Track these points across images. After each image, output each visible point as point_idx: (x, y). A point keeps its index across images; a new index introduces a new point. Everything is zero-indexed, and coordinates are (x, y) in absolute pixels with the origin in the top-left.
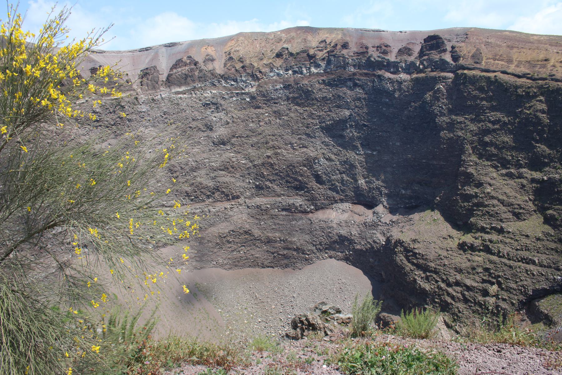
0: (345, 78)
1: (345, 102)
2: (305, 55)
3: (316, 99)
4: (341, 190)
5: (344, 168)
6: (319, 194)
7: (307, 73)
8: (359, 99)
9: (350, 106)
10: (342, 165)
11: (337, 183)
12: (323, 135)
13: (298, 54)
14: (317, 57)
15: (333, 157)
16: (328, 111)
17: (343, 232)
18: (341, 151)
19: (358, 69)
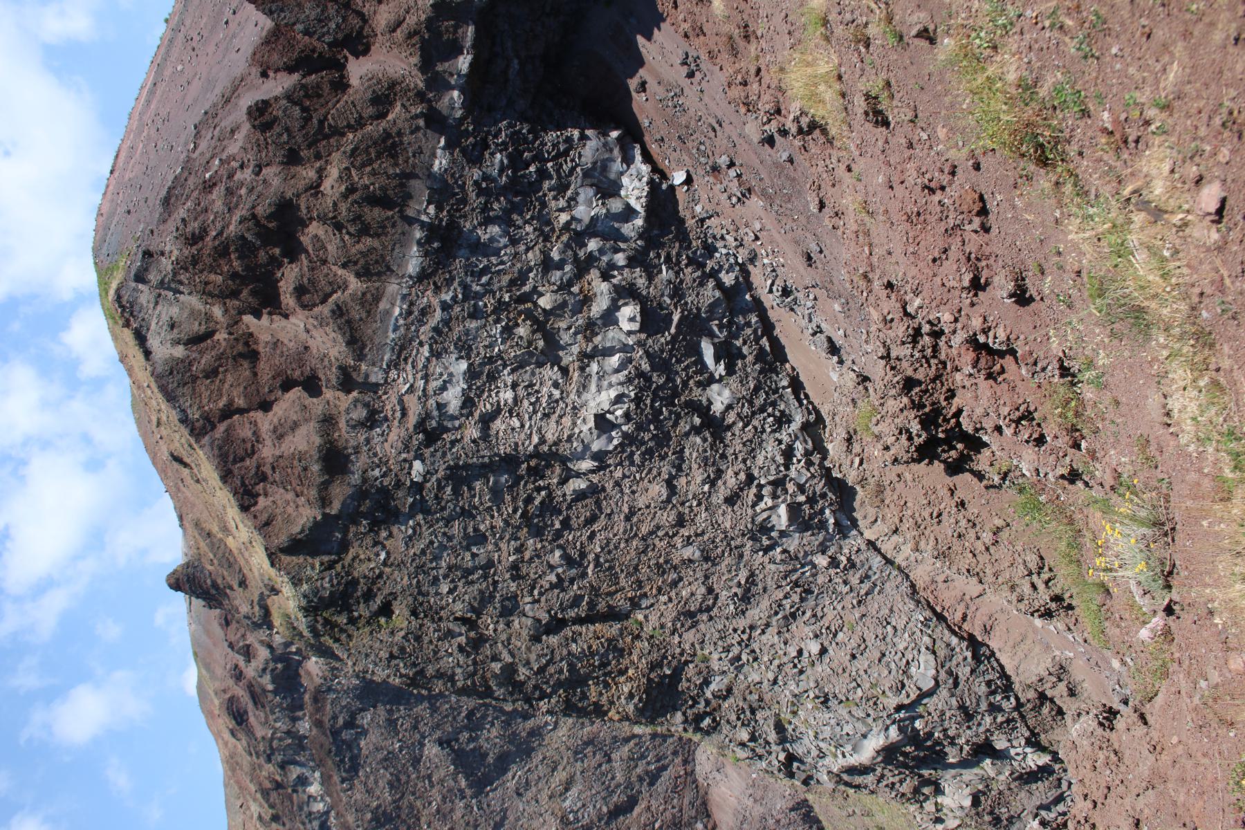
0: (330, 744)
1: (401, 751)
2: (274, 795)
3: (394, 802)
4: (658, 761)
5: (594, 754)
6: (665, 810)
7: (322, 800)
8: (391, 723)
9: (413, 744)
10: (585, 756)
11: (639, 770)
12: (499, 792)
13: (272, 806)
14: (278, 778)
15: (561, 776)
16: (430, 781)
17: (781, 805)
18: (544, 758)
19: (301, 708)
